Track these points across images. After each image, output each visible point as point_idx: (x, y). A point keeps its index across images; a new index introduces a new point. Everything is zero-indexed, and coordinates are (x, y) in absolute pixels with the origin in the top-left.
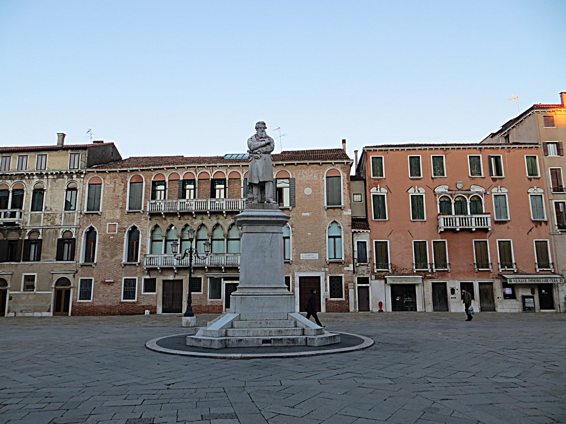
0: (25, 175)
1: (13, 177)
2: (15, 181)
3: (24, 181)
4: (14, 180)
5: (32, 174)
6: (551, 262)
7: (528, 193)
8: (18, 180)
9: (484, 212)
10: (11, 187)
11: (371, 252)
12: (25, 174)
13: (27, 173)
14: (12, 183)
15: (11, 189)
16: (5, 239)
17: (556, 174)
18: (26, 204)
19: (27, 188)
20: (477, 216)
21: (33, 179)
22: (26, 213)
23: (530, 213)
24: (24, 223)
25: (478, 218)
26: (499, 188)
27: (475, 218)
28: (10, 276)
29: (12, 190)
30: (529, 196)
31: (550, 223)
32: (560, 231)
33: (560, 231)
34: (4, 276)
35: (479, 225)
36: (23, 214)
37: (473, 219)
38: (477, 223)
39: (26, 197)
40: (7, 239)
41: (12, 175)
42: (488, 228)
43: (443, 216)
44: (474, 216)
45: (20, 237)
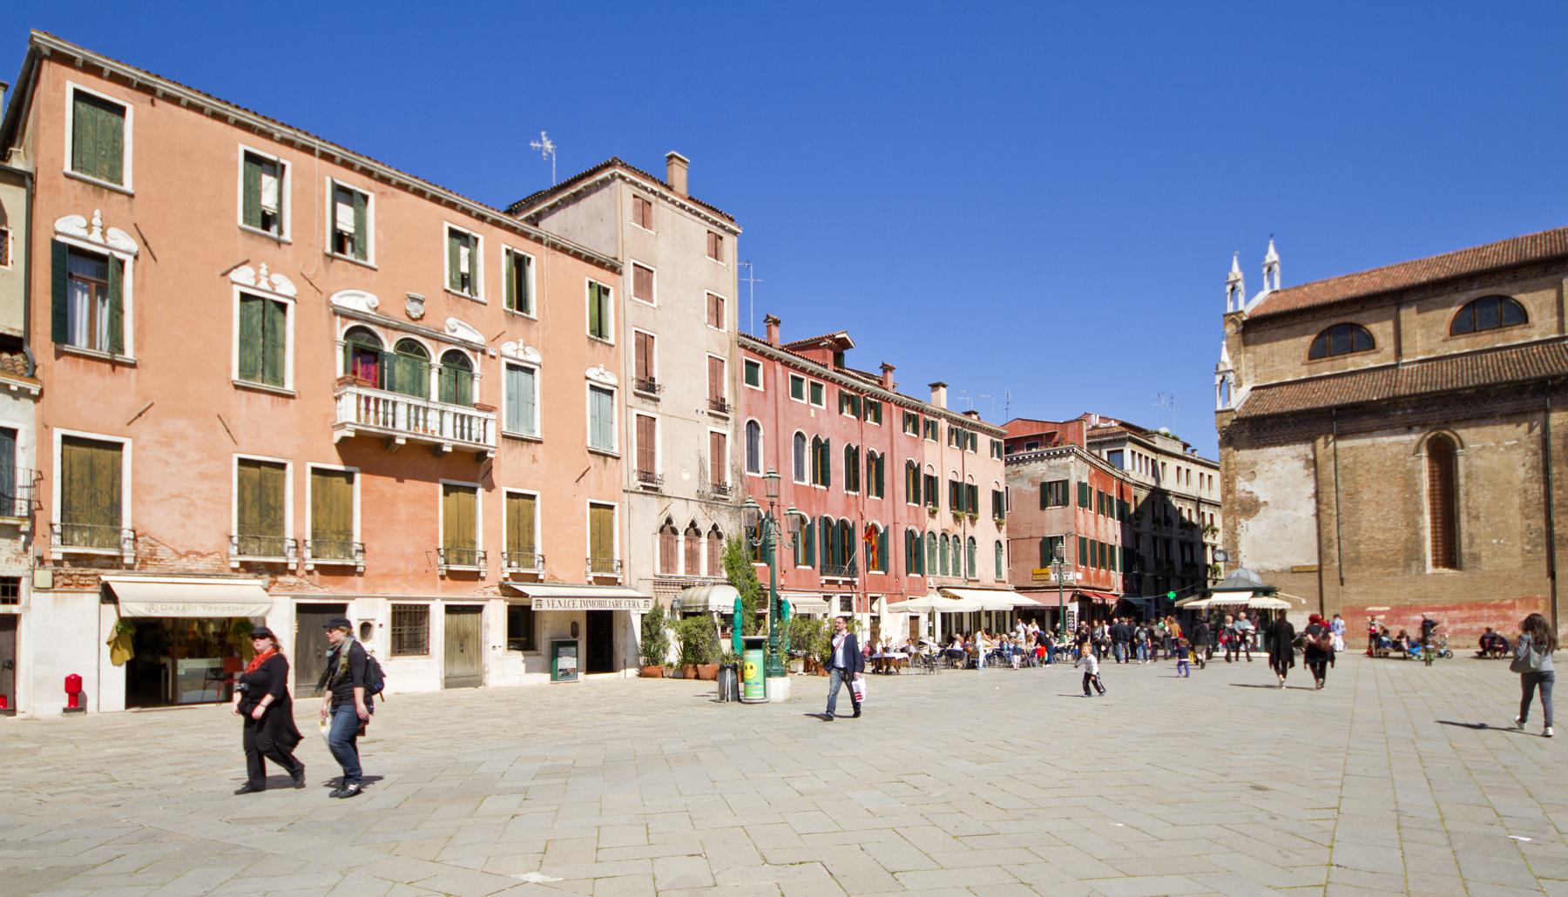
6: (617, 557)
7: (587, 378)
9: (476, 400)
11: (40, 478)
17: (645, 344)
20: (461, 410)
23: (585, 431)
25: (462, 417)
26: (521, 346)
27: (455, 415)
30: (588, 387)
31: (624, 460)
32: (642, 486)
33: (642, 486)
35: (462, 436)
37: (448, 419)
38: (458, 430)
42: (485, 453)
43: (354, 389)
44: (452, 408)
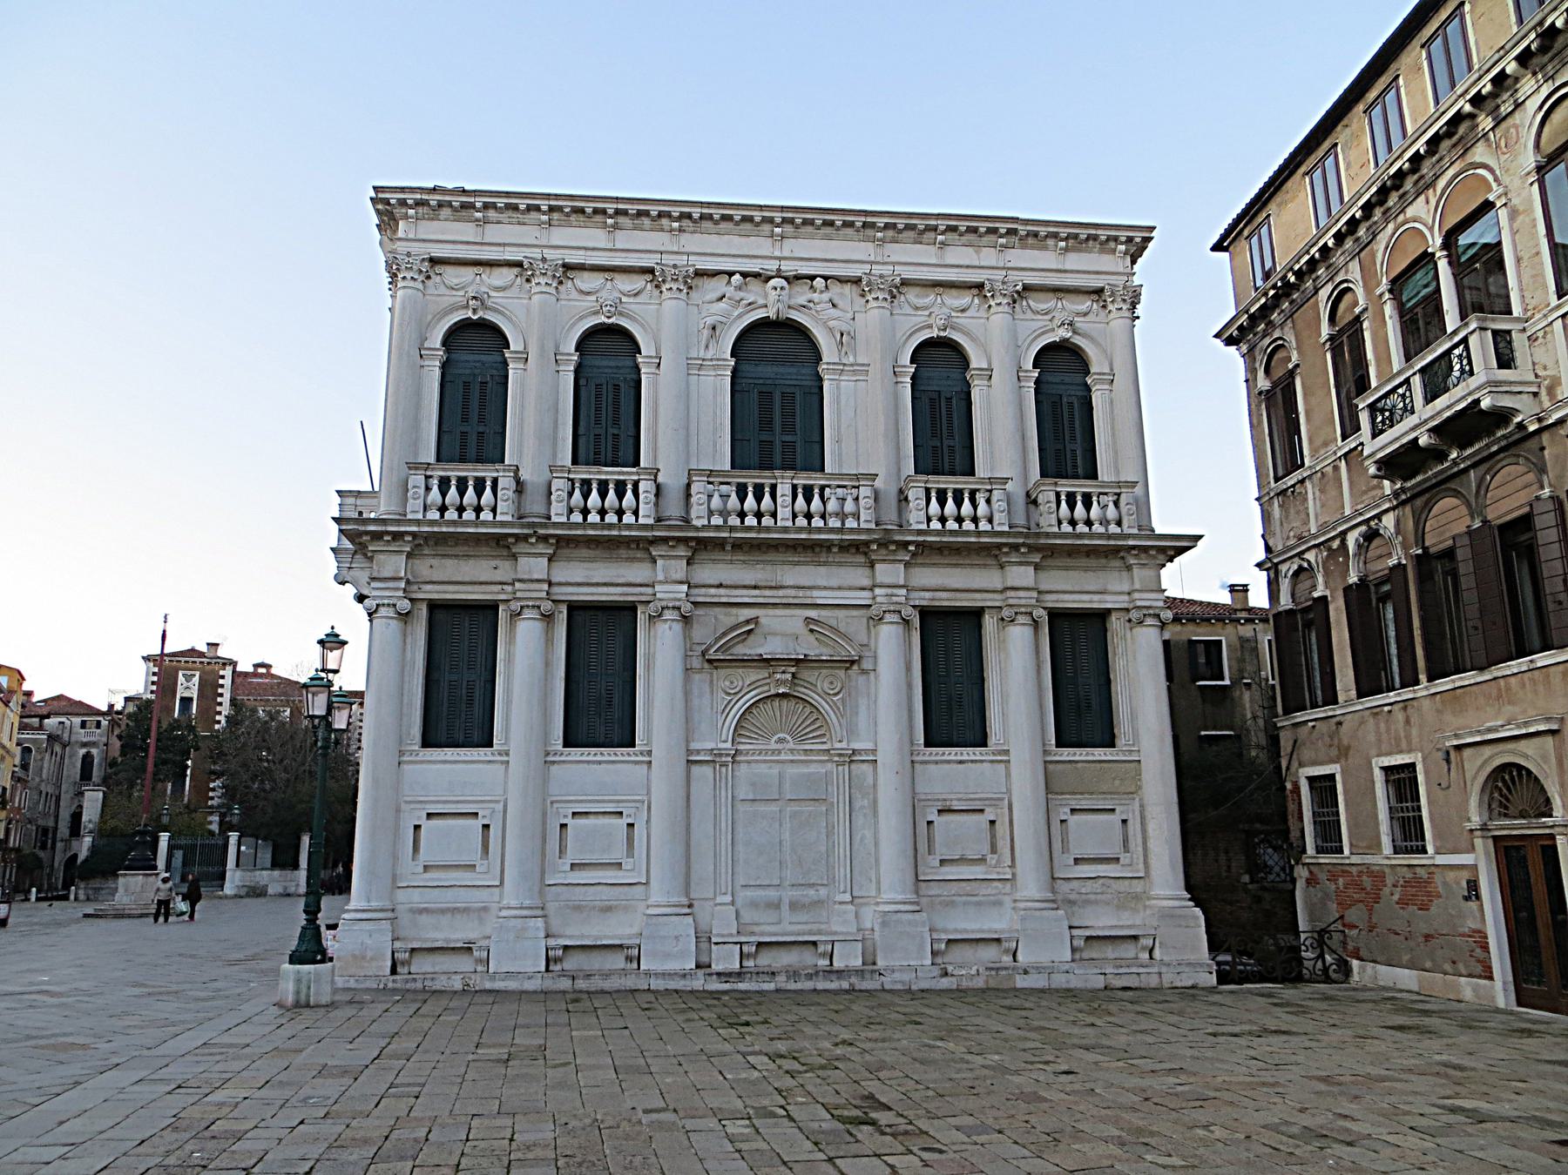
0: (1472, 116)
1: (1426, 168)
2: (1441, 183)
3: (1479, 153)
4: (1432, 184)
5: (1500, 80)
8: (1451, 172)
10: (1431, 229)
12: (1468, 108)
13: (1473, 92)
14: (1433, 202)
15: (1435, 242)
16: (1477, 524)
18: (1526, 279)
19: (1506, 180)
21: (1518, 105)
22: (1534, 328)
24: (1543, 392)
28: (1549, 739)
29: (1439, 241)
34: (1523, 745)
36: (1518, 340)
39: (1514, 233)
40: (1485, 522)
41: (1417, 159)
45: (1542, 487)
